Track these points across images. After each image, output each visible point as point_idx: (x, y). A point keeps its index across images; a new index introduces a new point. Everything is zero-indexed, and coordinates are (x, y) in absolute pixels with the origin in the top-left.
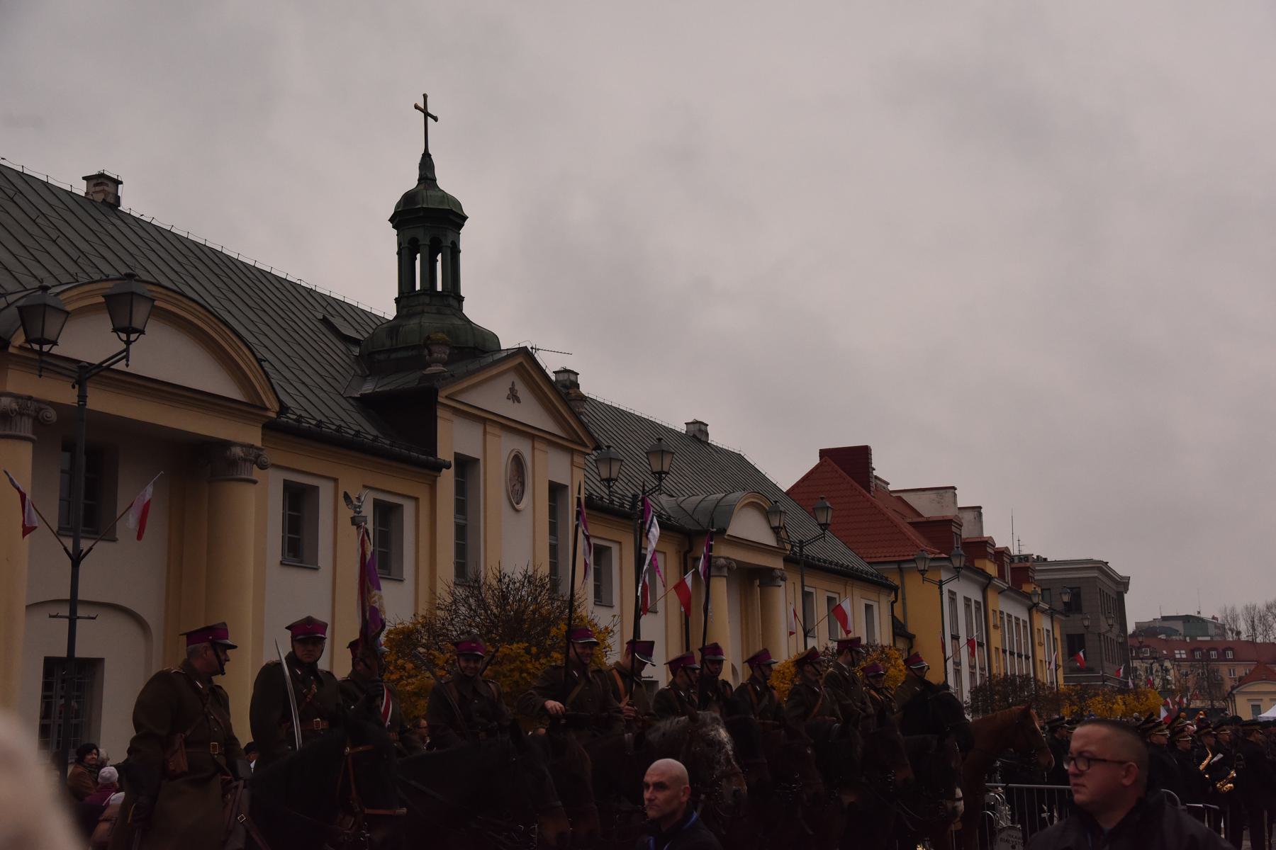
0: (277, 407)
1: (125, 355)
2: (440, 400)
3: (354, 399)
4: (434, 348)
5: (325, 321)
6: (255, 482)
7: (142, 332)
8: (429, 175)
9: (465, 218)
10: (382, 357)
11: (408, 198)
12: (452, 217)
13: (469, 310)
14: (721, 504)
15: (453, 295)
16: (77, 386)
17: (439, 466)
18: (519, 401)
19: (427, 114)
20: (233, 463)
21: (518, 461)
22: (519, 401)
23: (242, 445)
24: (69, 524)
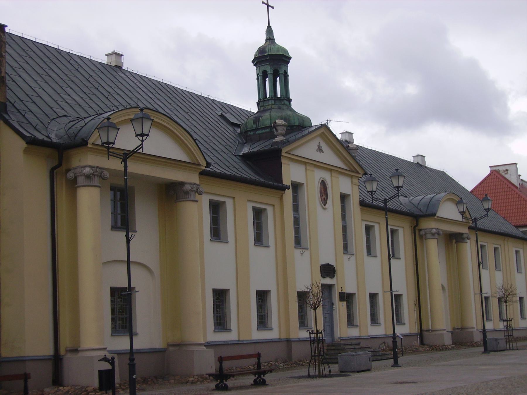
0: (205, 164)
1: (141, 146)
2: (282, 154)
3: (240, 156)
4: (278, 128)
5: (222, 116)
6: (197, 201)
7: (148, 135)
8: (272, 37)
9: (290, 58)
10: (252, 133)
11: (261, 50)
12: (284, 58)
13: (294, 106)
14: (433, 200)
15: (286, 99)
16: (123, 162)
17: (284, 188)
18: (323, 152)
19: (268, 6)
20: (187, 193)
21: (323, 184)
22: (323, 152)
23: (191, 184)
24: (115, 225)
